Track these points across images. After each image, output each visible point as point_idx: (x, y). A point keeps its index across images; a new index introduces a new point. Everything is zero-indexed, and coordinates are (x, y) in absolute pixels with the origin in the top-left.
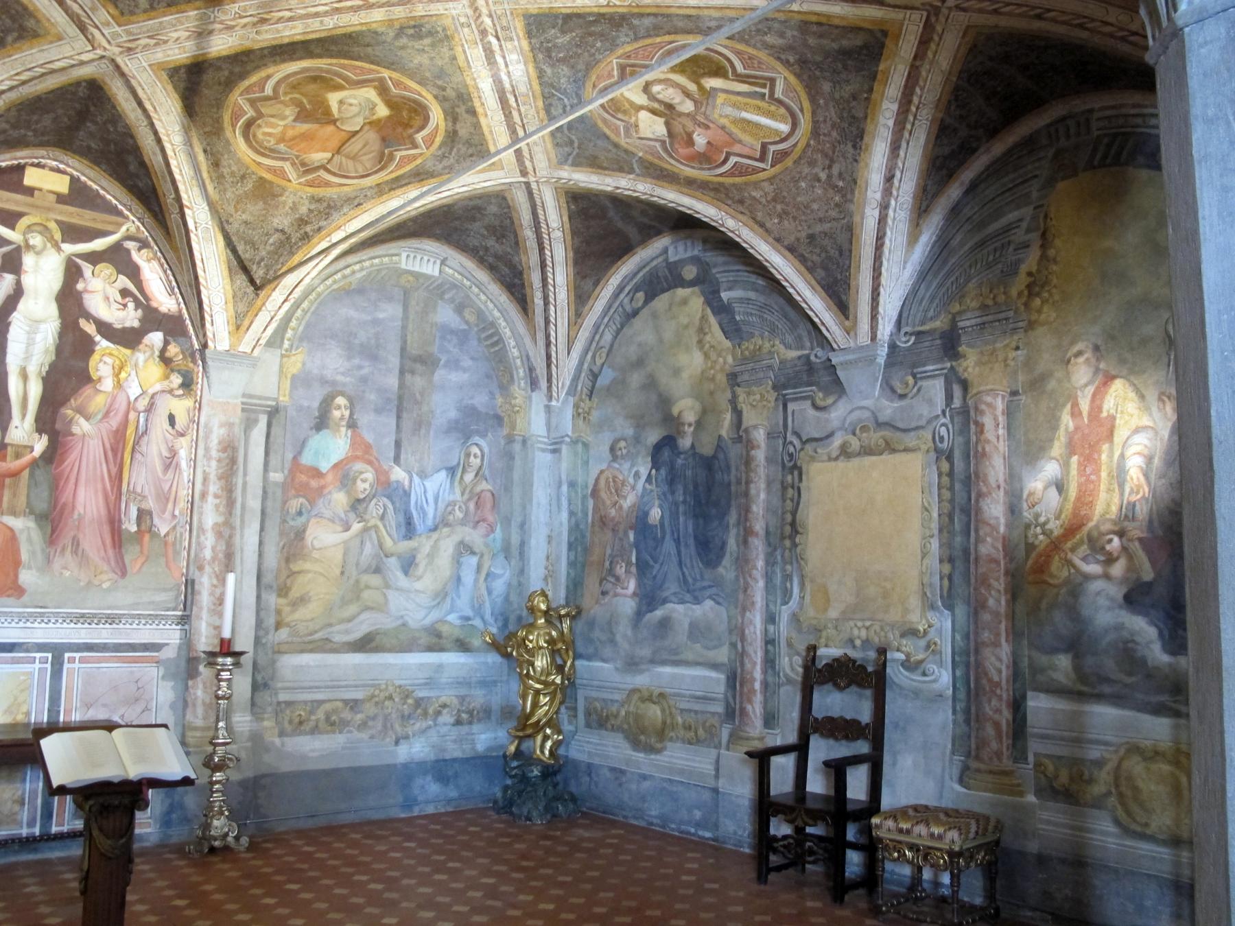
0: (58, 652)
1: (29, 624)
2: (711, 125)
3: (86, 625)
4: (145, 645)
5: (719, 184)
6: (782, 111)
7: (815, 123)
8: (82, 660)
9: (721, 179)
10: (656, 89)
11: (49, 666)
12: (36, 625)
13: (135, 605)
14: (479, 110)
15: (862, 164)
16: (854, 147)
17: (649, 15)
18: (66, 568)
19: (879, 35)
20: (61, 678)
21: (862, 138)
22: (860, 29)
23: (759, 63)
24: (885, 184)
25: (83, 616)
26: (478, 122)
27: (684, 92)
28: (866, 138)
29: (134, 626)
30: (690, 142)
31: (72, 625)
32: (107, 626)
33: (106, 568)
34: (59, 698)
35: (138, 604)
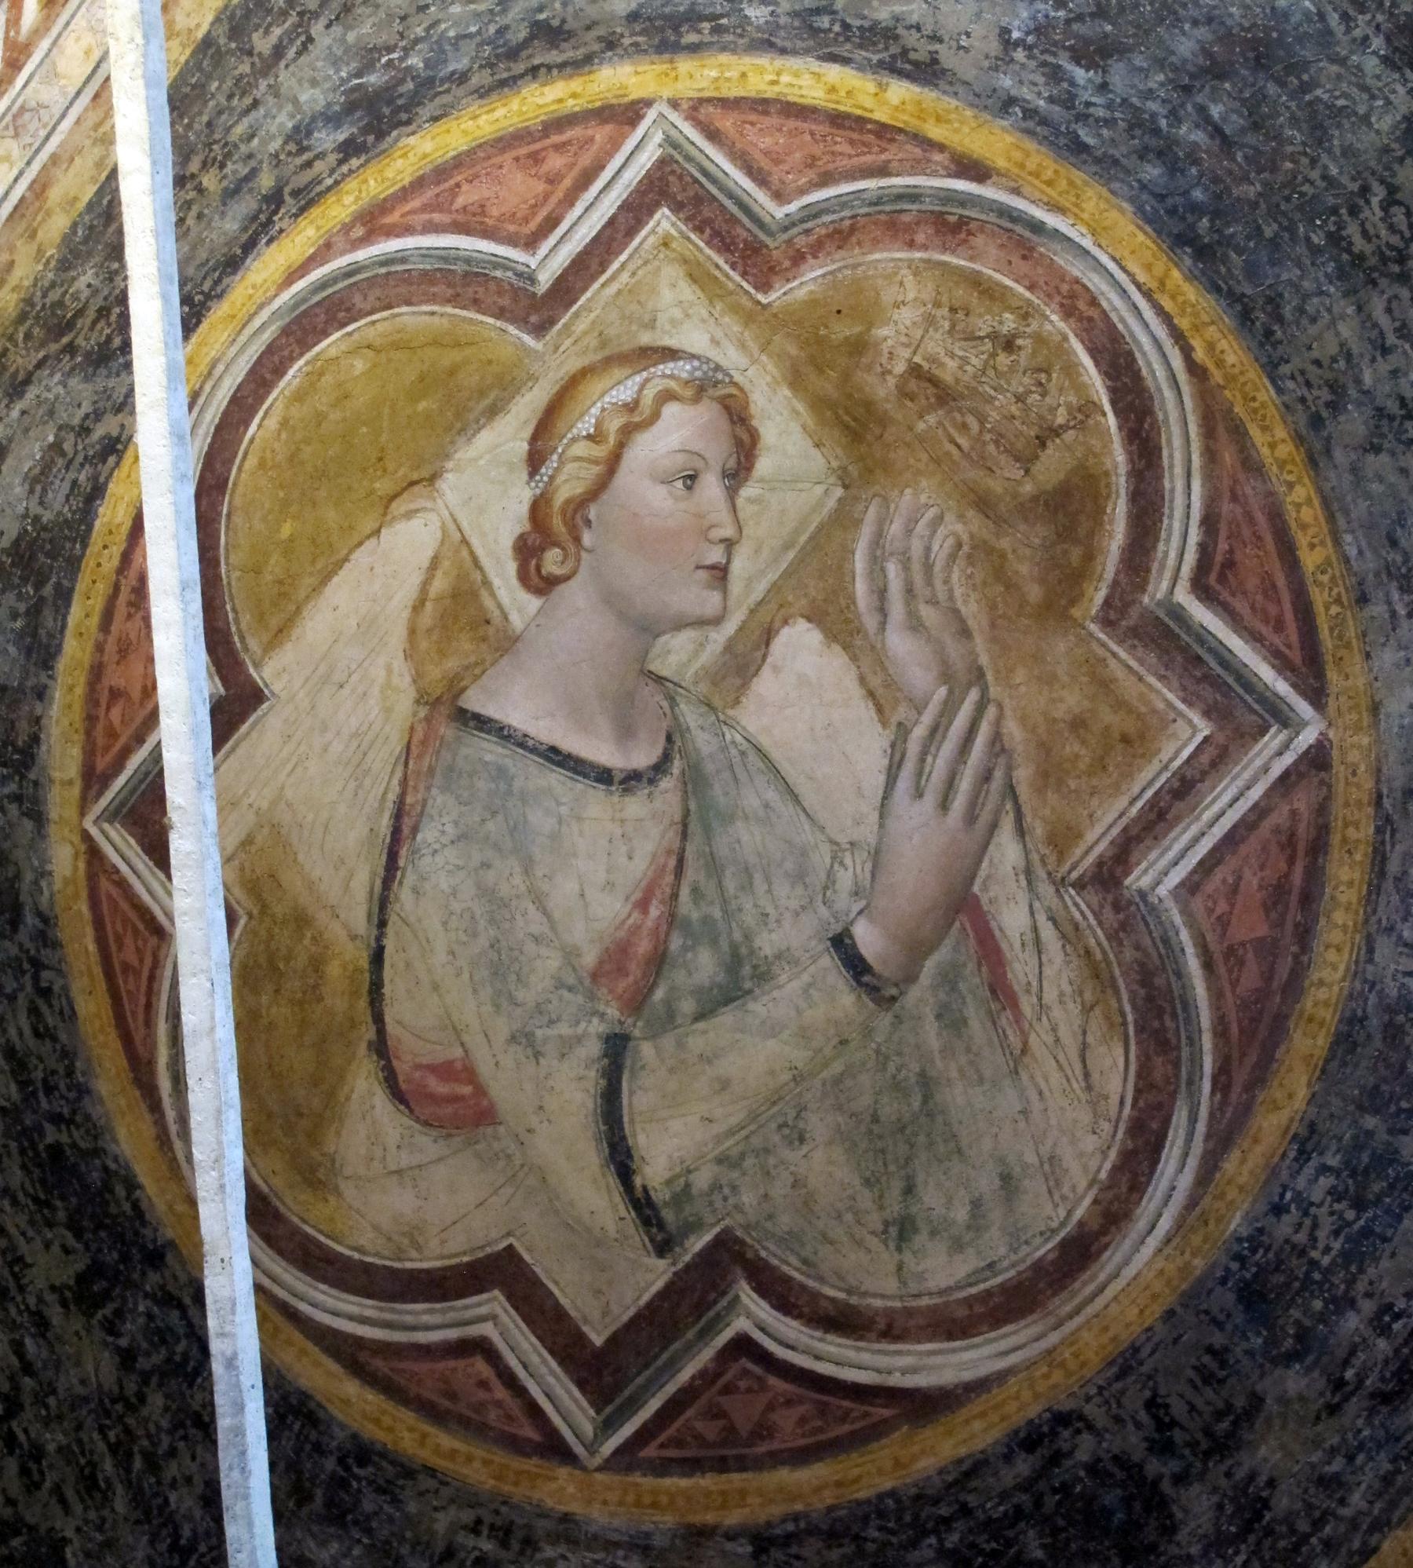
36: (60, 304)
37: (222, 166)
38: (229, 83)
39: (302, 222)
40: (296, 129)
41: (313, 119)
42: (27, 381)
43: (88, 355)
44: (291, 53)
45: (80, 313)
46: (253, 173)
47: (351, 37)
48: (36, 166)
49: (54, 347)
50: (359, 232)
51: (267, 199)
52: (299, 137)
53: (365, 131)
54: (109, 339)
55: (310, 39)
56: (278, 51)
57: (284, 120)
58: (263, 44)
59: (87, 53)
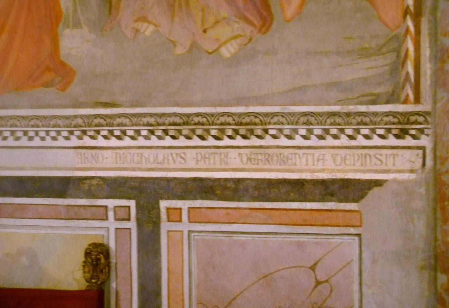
0: (147, 194)
1: (87, 141)
3: (196, 142)
4: (323, 183)
8: (195, 216)
11: (132, 225)
12: (101, 142)
13: (298, 93)
18: (143, 19)
20: (157, 252)
25: (187, 120)
29: (298, 141)
31: (168, 141)
32: (239, 141)
33: (225, 12)
34: (158, 294)
35: (303, 89)
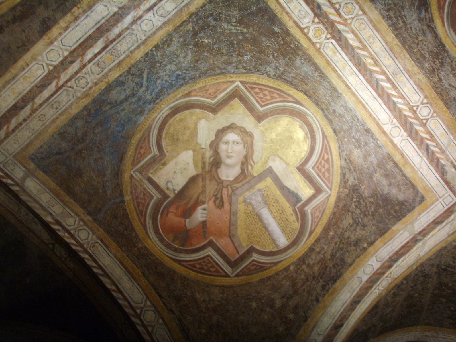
2: (226, 206)
5: (172, 272)
6: (297, 226)
7: (311, 250)
9: (176, 267)
10: (231, 136)
14: (55, 31)
15: (321, 305)
16: (324, 287)
17: (315, 65)
19: (418, 199)
21: (335, 281)
22: (413, 186)
23: (328, 170)
24: (331, 330)
26: (33, 43)
27: (246, 157)
28: (337, 284)
30: (188, 212)
36: (429, 70)
37: (419, 36)
38: (405, 32)
39: (435, 21)
40: (419, 20)
41: (418, 17)
42: (440, 78)
43: (441, 66)
44: (405, 19)
45: (432, 67)
46: (423, 30)
47: (407, 7)
48: (404, 72)
49: (436, 73)
50: (441, 11)
51: (428, 28)
52: (420, 20)
53: (425, 6)
54: (439, 62)
55: (404, 15)
56: (404, 22)
57: (416, 23)
58: (401, 24)
59: (388, 59)
